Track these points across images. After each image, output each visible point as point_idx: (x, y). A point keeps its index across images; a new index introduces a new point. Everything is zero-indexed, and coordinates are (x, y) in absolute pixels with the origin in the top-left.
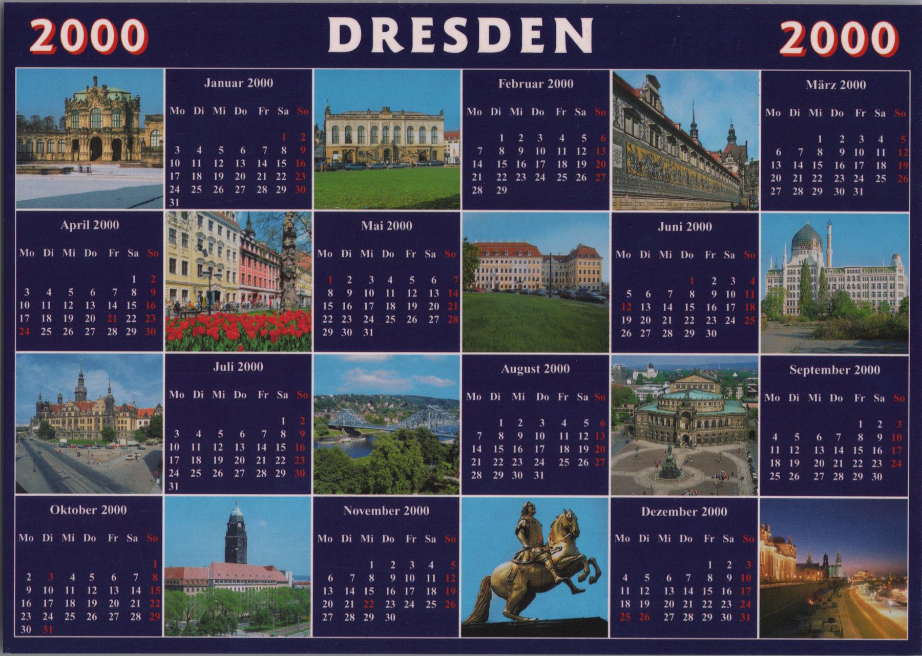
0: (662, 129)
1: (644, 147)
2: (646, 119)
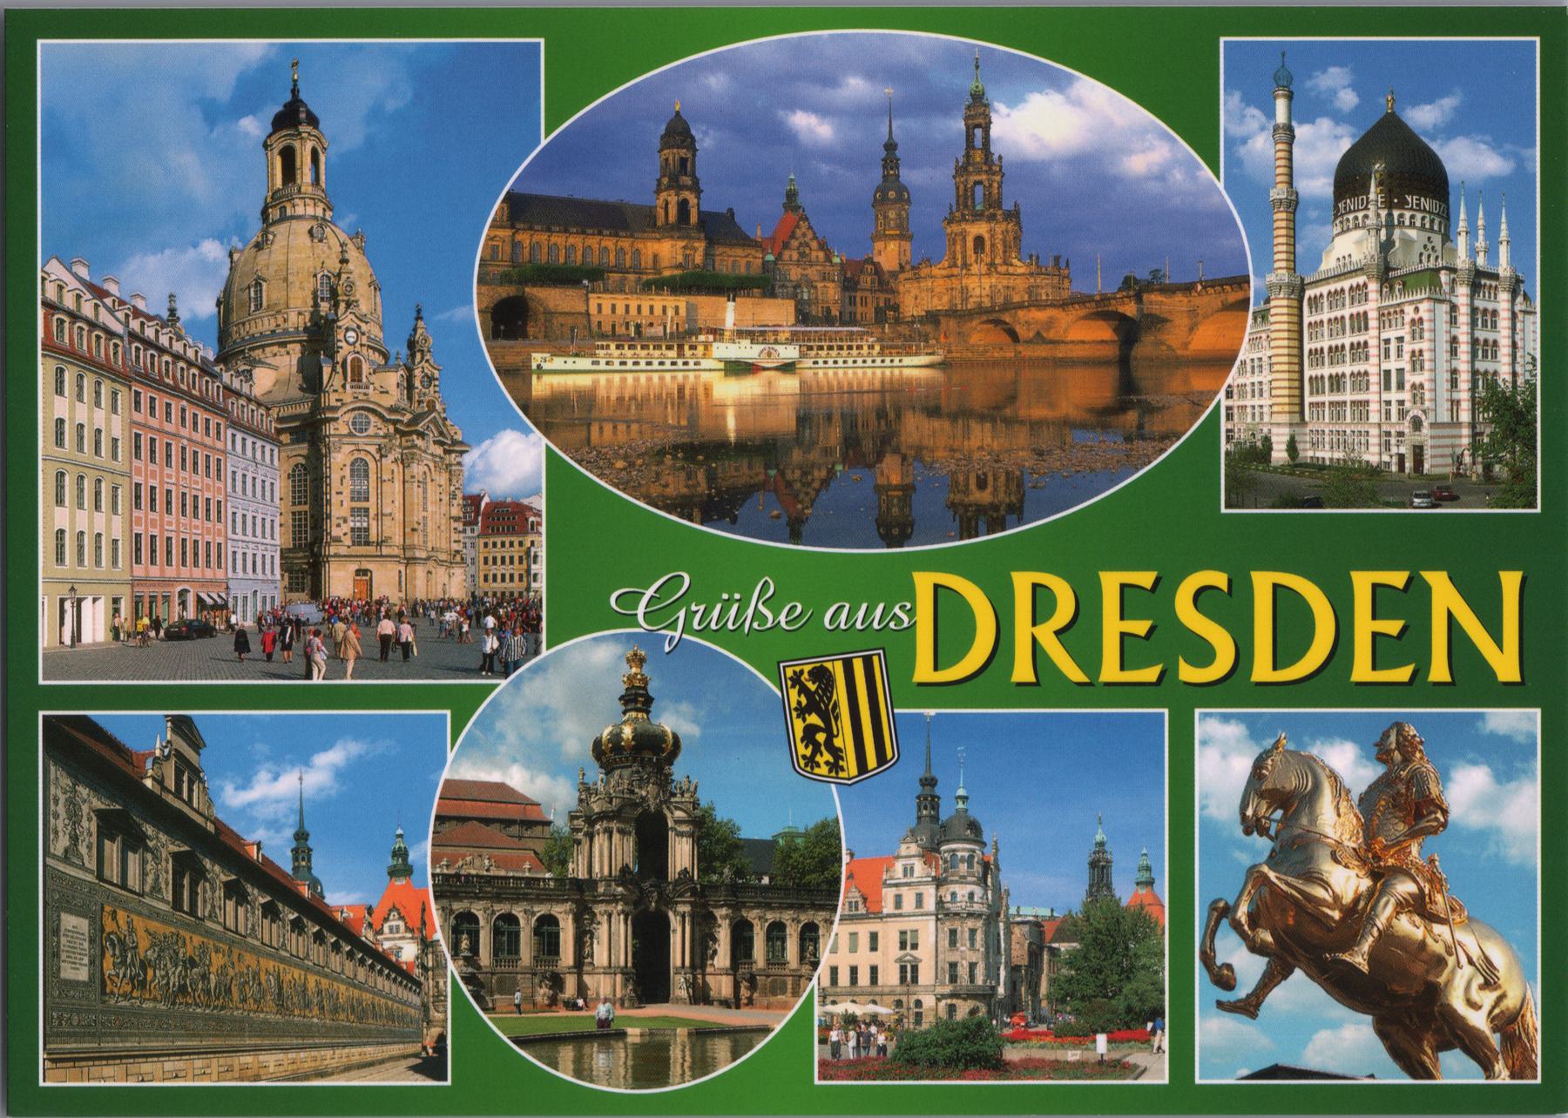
0: (208, 864)
1: (155, 915)
2: (163, 837)
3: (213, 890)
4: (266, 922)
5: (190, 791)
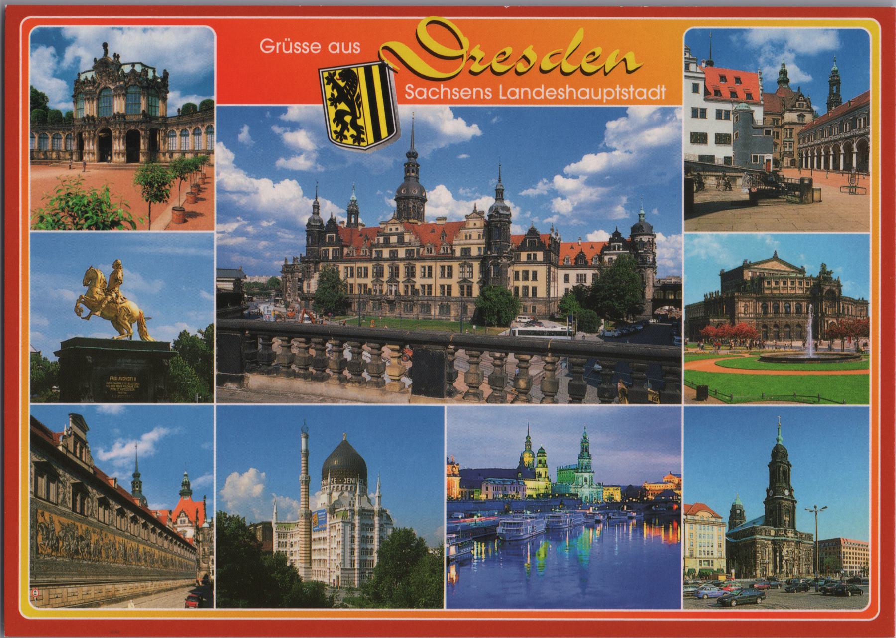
0: (89, 488)
1: (64, 514)
2: (67, 475)
3: (92, 502)
4: (119, 518)
5: (81, 452)
